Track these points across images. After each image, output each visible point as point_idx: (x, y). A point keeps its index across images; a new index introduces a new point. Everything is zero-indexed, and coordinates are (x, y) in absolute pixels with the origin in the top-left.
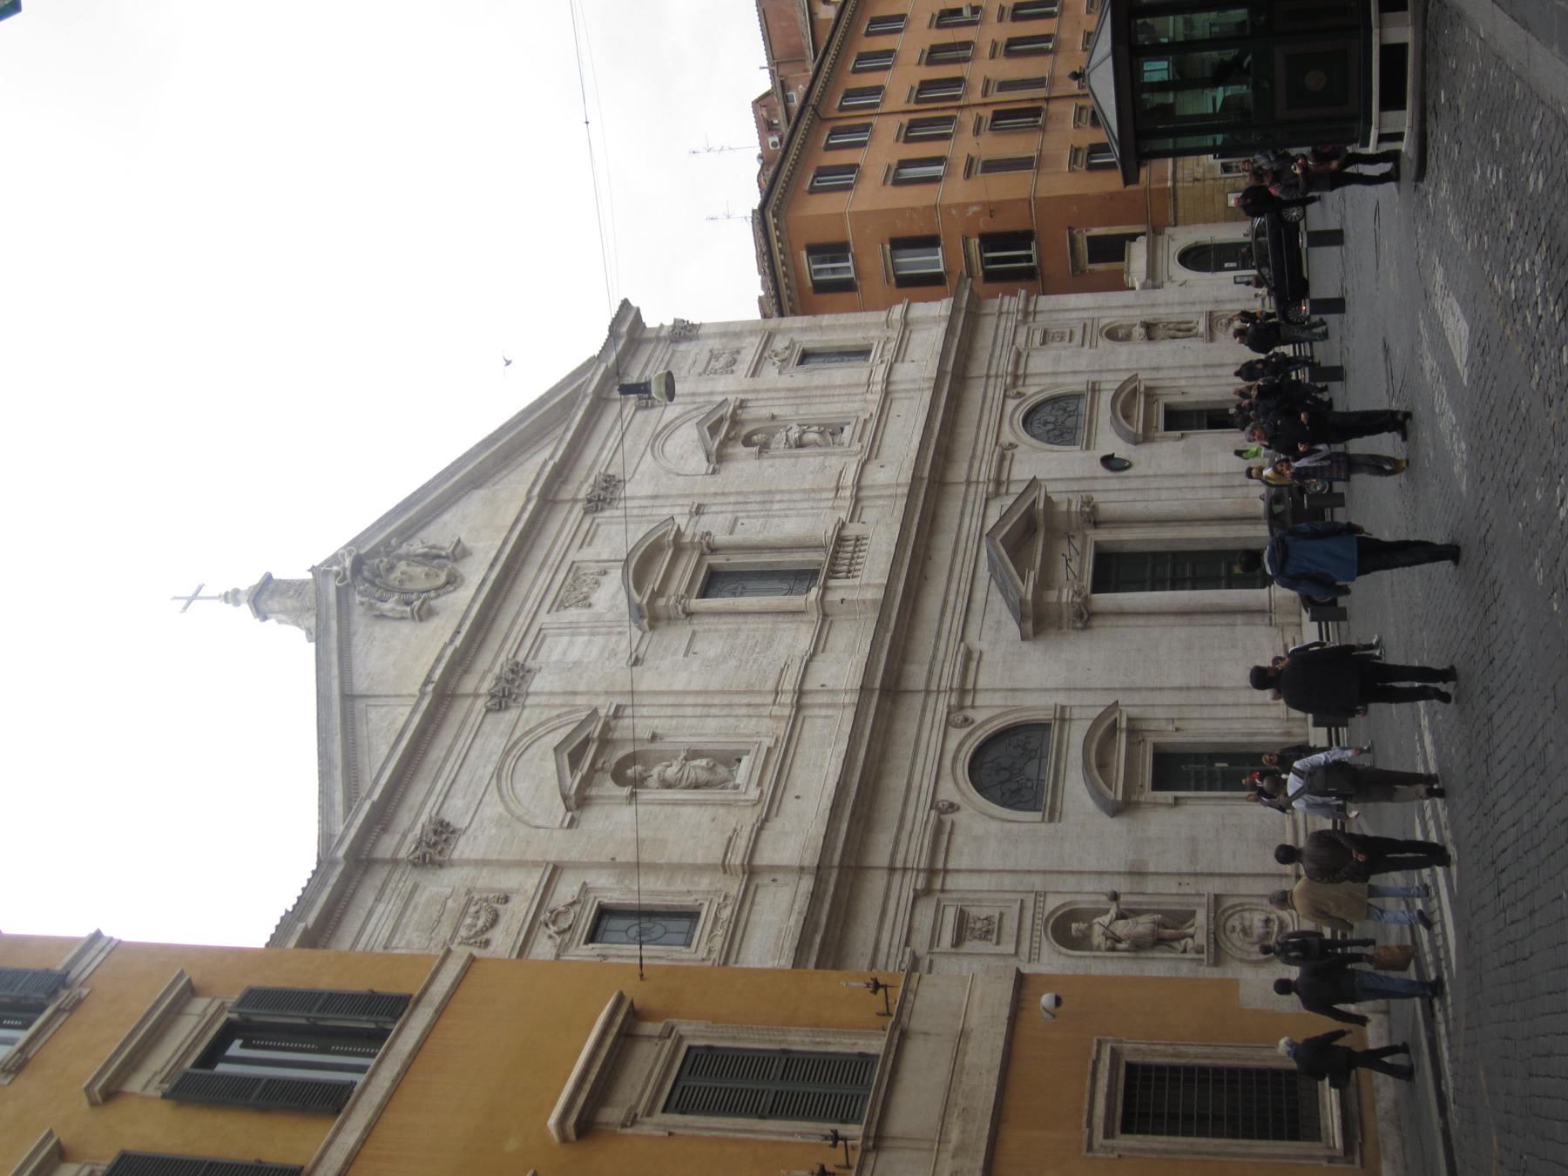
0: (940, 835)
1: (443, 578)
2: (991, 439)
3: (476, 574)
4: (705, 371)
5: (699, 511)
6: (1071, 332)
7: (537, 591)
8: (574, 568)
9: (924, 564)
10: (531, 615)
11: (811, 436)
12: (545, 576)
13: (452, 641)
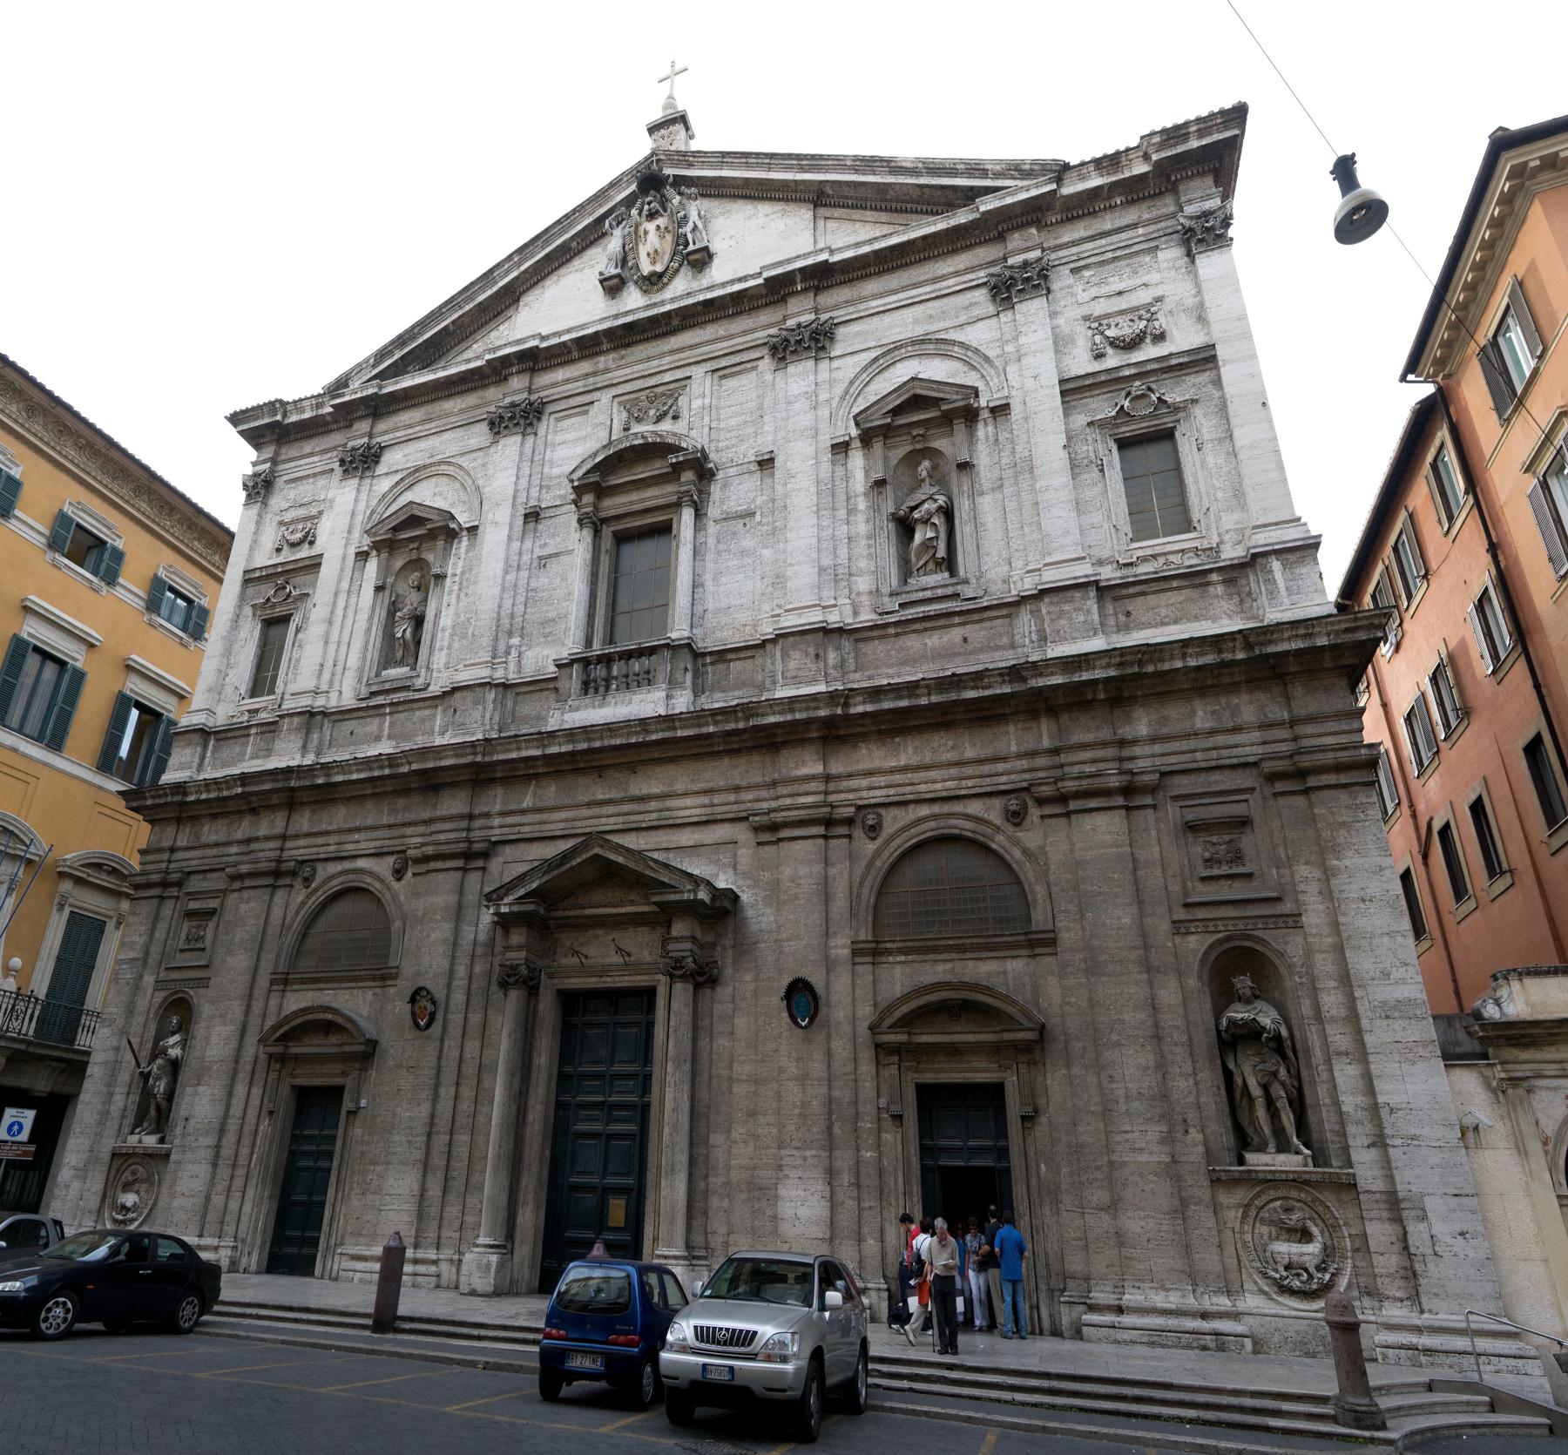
0: (279, 875)
2: (878, 796)
3: (682, 290)
6: (1249, 876)
8: (683, 383)
9: (618, 766)
13: (543, 338)
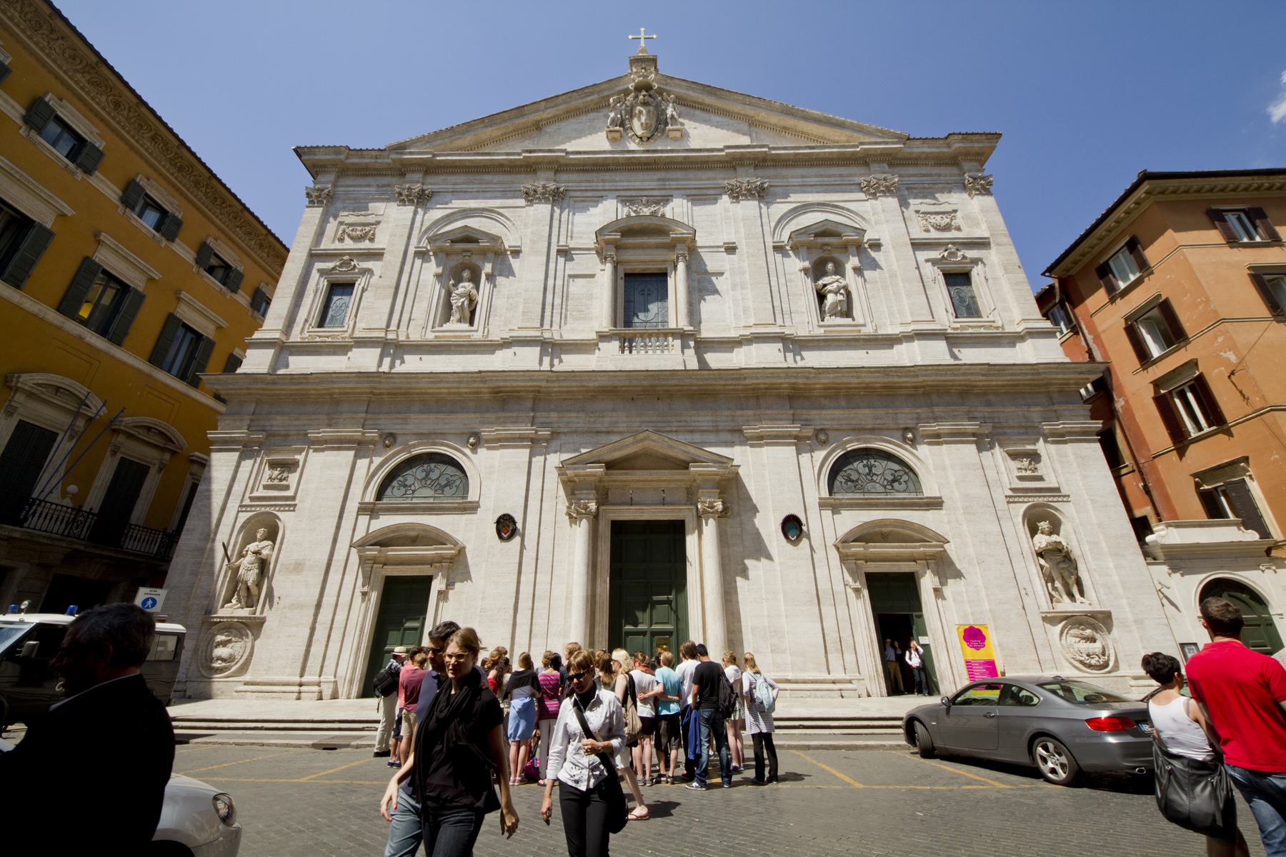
1: (639, 133)
4: (923, 213)
5: (731, 249)
7: (637, 185)
10: (613, 188)
11: (831, 299)
12: (654, 184)
